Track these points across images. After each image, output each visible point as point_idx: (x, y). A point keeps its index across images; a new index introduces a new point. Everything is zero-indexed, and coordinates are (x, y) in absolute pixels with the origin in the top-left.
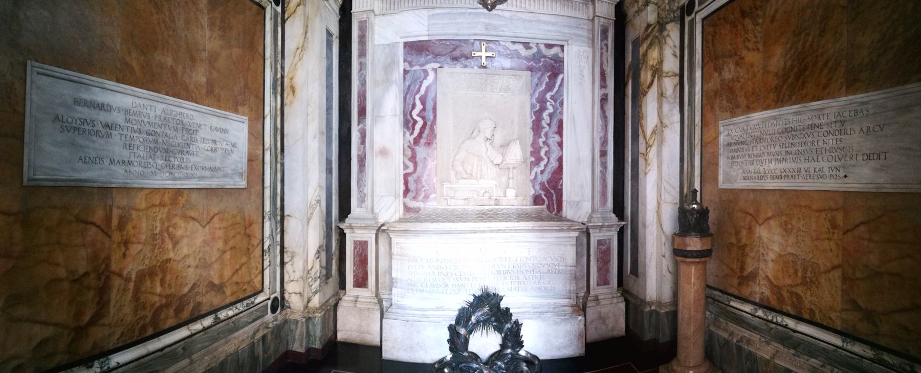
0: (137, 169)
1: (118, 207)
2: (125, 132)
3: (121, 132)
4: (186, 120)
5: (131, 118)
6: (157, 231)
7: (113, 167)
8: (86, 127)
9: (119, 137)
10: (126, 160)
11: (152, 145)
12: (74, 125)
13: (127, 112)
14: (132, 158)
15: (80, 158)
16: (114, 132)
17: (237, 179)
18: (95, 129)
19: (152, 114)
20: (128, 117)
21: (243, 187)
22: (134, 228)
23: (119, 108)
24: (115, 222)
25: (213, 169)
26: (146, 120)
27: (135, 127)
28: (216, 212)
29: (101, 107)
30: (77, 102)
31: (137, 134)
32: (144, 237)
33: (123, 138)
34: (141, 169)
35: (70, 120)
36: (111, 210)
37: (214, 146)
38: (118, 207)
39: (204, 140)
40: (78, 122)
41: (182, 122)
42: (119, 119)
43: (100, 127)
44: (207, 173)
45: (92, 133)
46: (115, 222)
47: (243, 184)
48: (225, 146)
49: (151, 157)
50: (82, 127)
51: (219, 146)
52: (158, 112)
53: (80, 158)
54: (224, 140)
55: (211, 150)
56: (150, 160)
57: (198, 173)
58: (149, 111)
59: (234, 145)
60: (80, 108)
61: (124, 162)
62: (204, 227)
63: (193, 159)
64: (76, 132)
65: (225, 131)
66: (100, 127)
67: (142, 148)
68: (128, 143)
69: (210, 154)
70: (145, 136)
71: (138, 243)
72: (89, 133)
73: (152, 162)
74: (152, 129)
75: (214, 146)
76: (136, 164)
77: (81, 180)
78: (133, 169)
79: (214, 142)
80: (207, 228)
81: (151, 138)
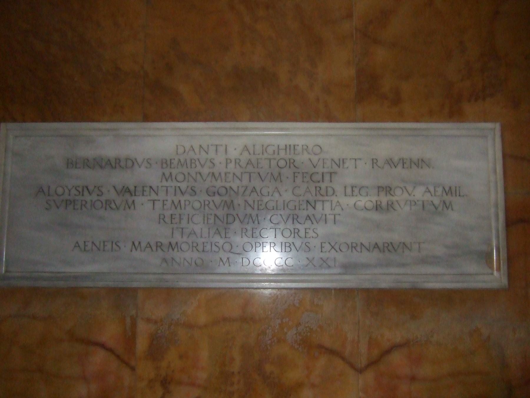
0: (188, 255)
1: (148, 320)
2: (162, 195)
3: (154, 196)
4: (303, 158)
5: (174, 172)
6: (236, 367)
7: (137, 254)
8: (87, 197)
9: (150, 205)
10: (165, 242)
11: (220, 213)
12: (66, 197)
13: (165, 163)
14: (177, 237)
15: (77, 245)
16: (139, 200)
17: (472, 267)
18: (103, 198)
19: (220, 158)
20: (167, 172)
21: (495, 285)
22: (181, 357)
23: (149, 162)
24: (142, 345)
25: (389, 247)
26: (206, 171)
27: (183, 186)
28: (398, 339)
29: (115, 164)
30: (71, 163)
31: (187, 197)
32: (202, 376)
33: (158, 205)
34: (196, 255)
35: (60, 191)
36: (134, 325)
37: (384, 199)
38: (148, 320)
39: (355, 190)
40: (74, 192)
41: (291, 163)
42: (152, 177)
43: (113, 195)
44: (364, 257)
45: (98, 204)
46: (142, 345)
47: (495, 277)
48: (419, 193)
49: (218, 232)
50: (80, 198)
51: (399, 196)
52: (233, 154)
53: (77, 245)
54: (416, 184)
55: (378, 207)
56: (217, 238)
57: (340, 258)
58: (212, 154)
59: (449, 191)
60: (75, 172)
61: (159, 245)
62: (360, 371)
63: (321, 229)
64: (71, 207)
65: (421, 163)
66: (113, 195)
67: (198, 219)
68: (168, 213)
69: (376, 216)
70: (204, 197)
71: (193, 384)
72: (93, 205)
73: (221, 242)
74: (219, 184)
75: (384, 199)
76: (184, 247)
77: (76, 277)
78: (177, 255)
79: (388, 190)
80: (369, 376)
81: (217, 199)
